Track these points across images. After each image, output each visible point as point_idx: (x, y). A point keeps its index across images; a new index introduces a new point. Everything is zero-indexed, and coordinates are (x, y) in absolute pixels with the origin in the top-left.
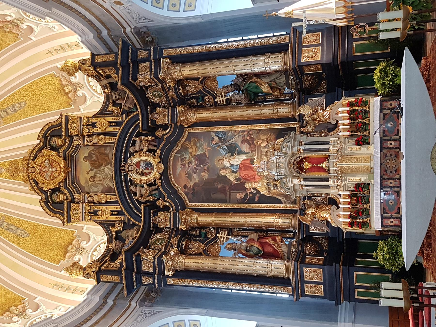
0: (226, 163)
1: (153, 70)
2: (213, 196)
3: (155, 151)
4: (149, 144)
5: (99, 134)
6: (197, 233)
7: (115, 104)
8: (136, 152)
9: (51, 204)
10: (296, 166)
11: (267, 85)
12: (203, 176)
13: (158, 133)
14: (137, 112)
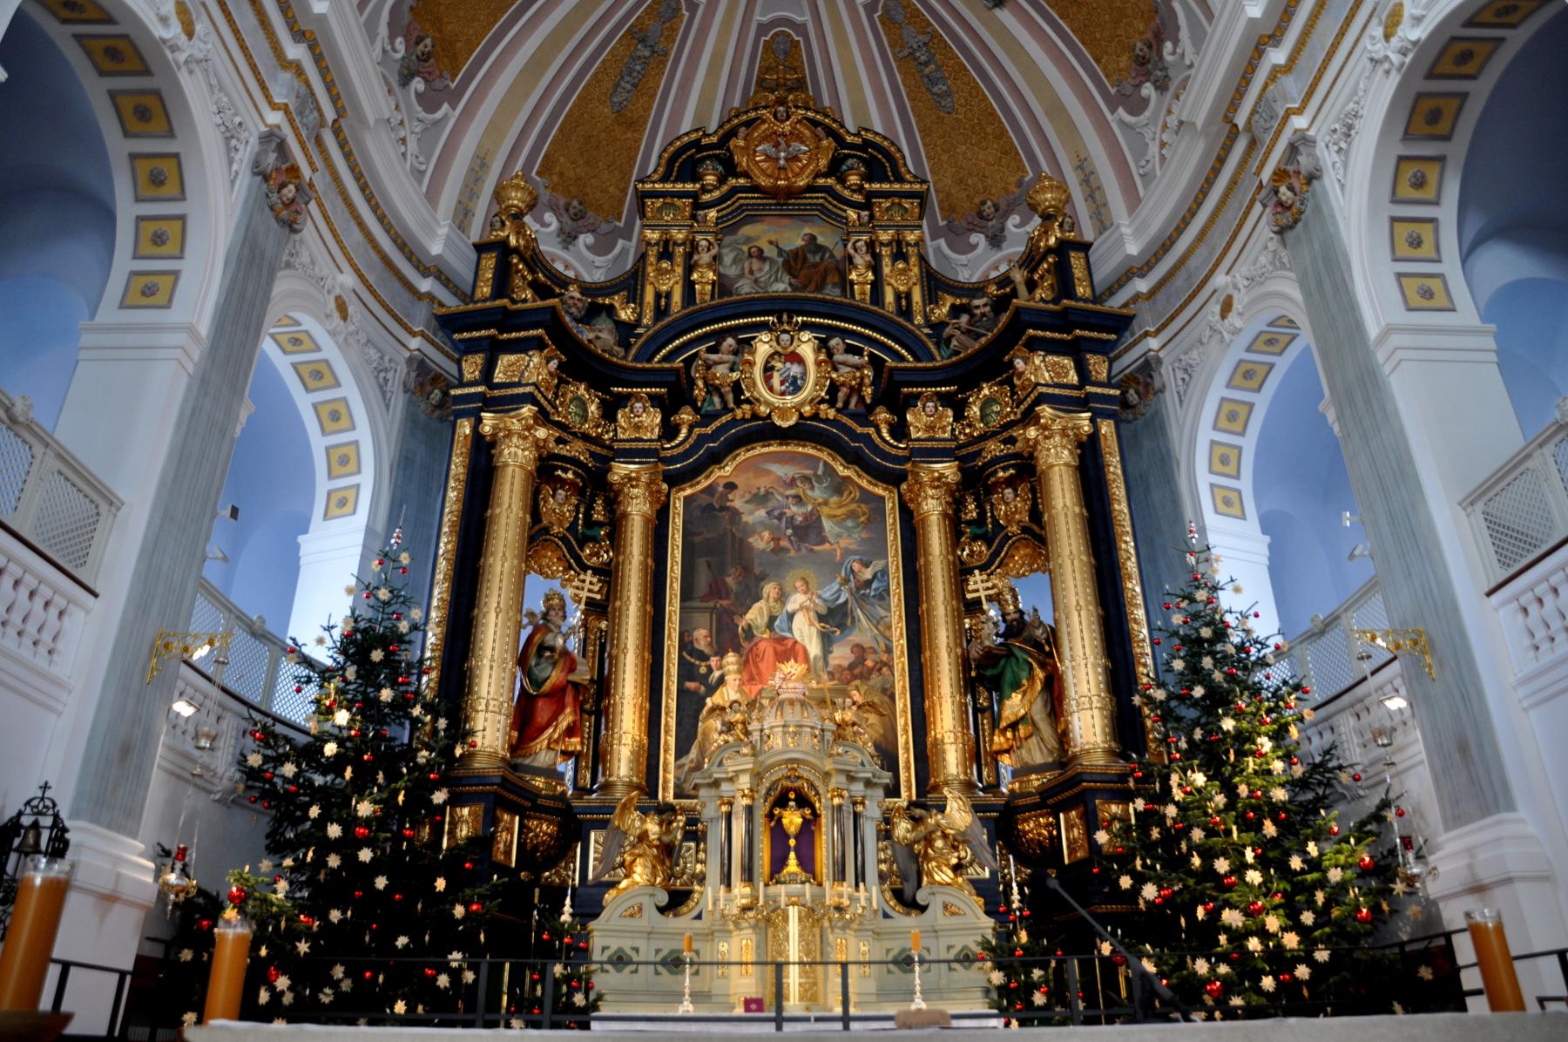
0: (796, 600)
1: (1057, 391)
2: (702, 565)
3: (832, 402)
4: (852, 388)
5: (876, 267)
6: (598, 516)
7: (956, 311)
8: (830, 354)
9: (692, 155)
10: (789, 784)
11: (1022, 712)
12: (759, 534)
13: (883, 415)
14: (938, 358)
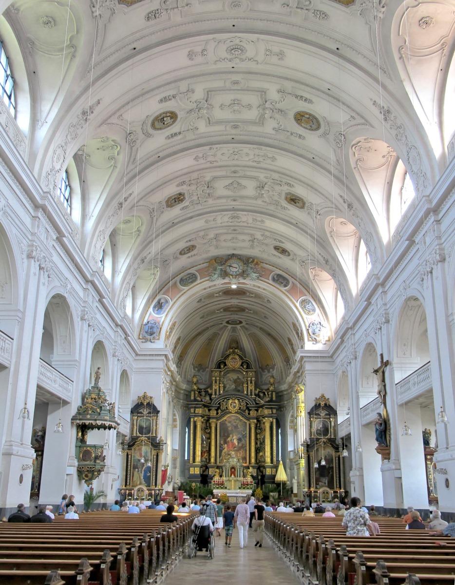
5: (247, 384)
13: (247, 411)
